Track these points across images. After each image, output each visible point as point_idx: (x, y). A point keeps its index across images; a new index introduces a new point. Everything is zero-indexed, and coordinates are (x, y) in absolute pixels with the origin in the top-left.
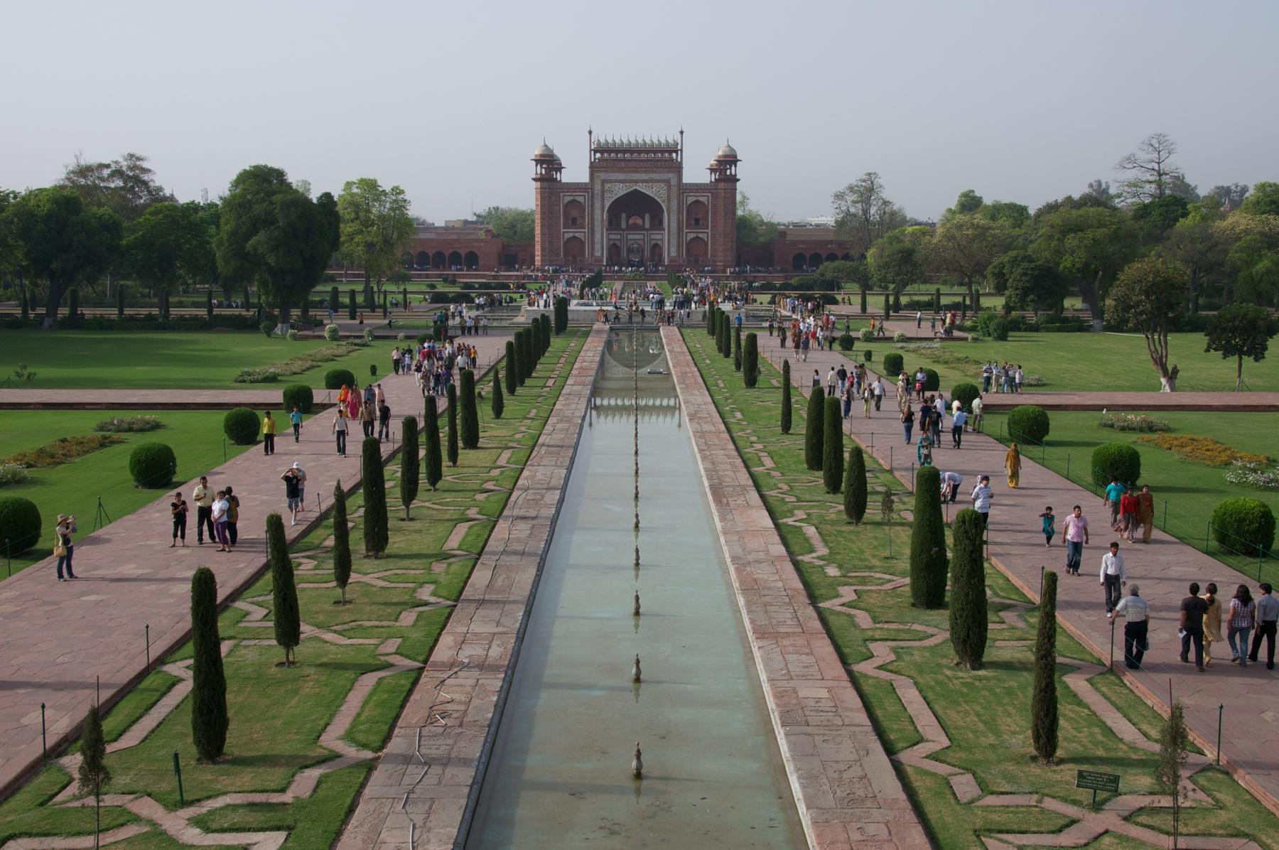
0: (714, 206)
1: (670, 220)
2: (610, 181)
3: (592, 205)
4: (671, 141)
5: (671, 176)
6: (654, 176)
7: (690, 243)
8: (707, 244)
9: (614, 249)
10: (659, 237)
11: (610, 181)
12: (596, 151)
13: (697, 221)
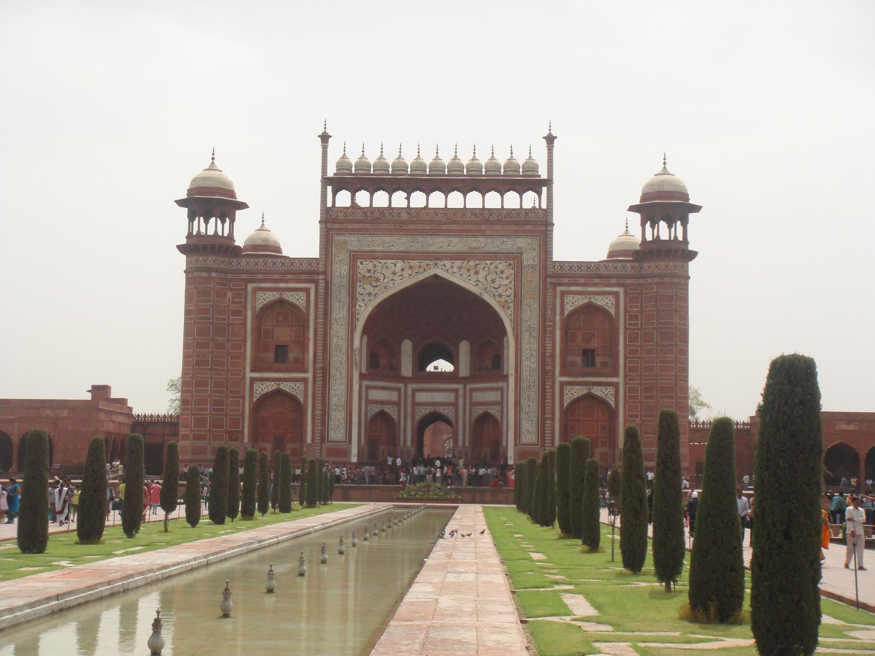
0: (631, 317)
1: (522, 353)
2: (371, 255)
3: (327, 312)
4: (521, 159)
5: (524, 243)
6: (481, 243)
7: (569, 411)
8: (612, 414)
9: (381, 426)
10: (493, 396)
11: (371, 255)
12: (337, 183)
13: (589, 356)
